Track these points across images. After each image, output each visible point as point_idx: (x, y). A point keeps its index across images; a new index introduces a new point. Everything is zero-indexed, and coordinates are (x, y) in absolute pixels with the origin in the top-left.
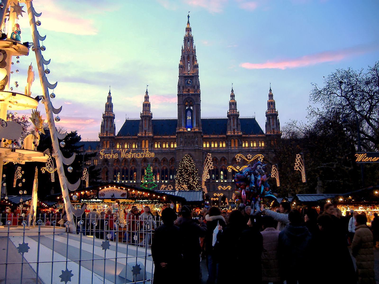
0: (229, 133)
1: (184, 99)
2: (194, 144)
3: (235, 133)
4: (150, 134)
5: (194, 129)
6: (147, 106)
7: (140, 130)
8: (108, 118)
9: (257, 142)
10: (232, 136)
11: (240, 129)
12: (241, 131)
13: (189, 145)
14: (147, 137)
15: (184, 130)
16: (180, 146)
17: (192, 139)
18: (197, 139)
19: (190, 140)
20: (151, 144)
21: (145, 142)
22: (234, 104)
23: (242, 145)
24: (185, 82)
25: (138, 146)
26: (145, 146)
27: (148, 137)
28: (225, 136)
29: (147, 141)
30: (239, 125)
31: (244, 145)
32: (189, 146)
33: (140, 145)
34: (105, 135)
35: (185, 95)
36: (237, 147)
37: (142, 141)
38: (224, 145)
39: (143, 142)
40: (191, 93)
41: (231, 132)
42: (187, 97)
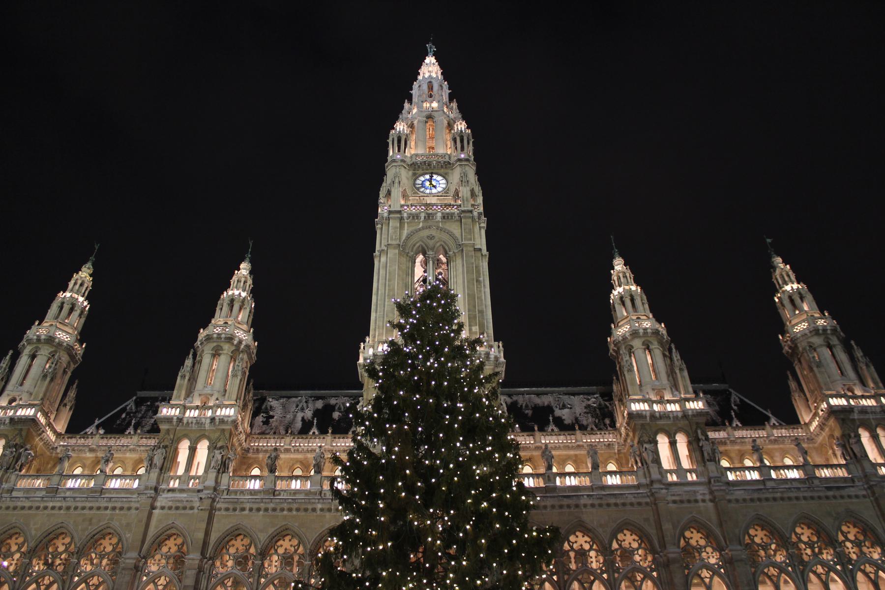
1: (405, 232)
7: (180, 390)
8: (40, 346)
14: (208, 421)
20: (219, 457)
21: (193, 450)
22: (635, 298)
24: (415, 180)
30: (681, 370)
33: (158, 460)
37: (179, 441)
42: (421, 225)
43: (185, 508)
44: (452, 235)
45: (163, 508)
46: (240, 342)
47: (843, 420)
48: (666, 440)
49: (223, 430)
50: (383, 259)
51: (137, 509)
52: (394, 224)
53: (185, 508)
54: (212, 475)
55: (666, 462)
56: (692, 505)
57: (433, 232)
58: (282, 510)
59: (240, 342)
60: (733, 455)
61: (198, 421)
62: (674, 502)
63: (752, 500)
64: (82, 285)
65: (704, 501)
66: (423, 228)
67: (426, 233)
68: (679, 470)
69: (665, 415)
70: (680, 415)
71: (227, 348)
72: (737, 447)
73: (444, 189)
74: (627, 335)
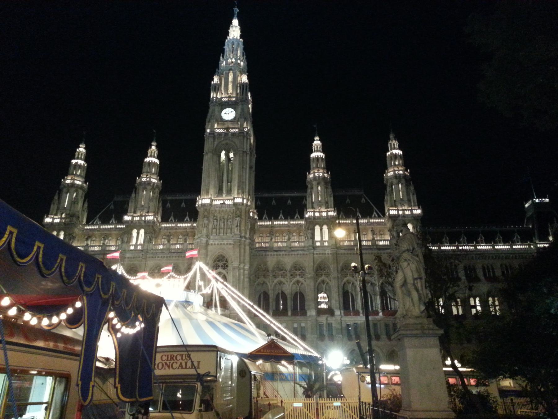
1: (216, 143)
2: (231, 230)
3: (322, 212)
5: (233, 200)
6: (152, 166)
12: (334, 208)
13: (222, 231)
14: (143, 222)
17: (227, 221)
18: (237, 219)
20: (148, 237)
21: (138, 234)
27: (145, 221)
29: (142, 232)
30: (330, 197)
32: (221, 234)
35: (220, 134)
37: (132, 230)
40: (231, 130)
41: (313, 210)
44: (235, 143)
45: (128, 258)
49: (149, 225)
52: (211, 140)
53: (136, 257)
55: (317, 238)
56: (324, 255)
57: (228, 141)
58: (173, 257)
61: (139, 221)
62: (317, 254)
63: (348, 254)
64: (82, 155)
65: (328, 254)
66: (223, 140)
68: (322, 241)
69: (319, 218)
70: (325, 218)
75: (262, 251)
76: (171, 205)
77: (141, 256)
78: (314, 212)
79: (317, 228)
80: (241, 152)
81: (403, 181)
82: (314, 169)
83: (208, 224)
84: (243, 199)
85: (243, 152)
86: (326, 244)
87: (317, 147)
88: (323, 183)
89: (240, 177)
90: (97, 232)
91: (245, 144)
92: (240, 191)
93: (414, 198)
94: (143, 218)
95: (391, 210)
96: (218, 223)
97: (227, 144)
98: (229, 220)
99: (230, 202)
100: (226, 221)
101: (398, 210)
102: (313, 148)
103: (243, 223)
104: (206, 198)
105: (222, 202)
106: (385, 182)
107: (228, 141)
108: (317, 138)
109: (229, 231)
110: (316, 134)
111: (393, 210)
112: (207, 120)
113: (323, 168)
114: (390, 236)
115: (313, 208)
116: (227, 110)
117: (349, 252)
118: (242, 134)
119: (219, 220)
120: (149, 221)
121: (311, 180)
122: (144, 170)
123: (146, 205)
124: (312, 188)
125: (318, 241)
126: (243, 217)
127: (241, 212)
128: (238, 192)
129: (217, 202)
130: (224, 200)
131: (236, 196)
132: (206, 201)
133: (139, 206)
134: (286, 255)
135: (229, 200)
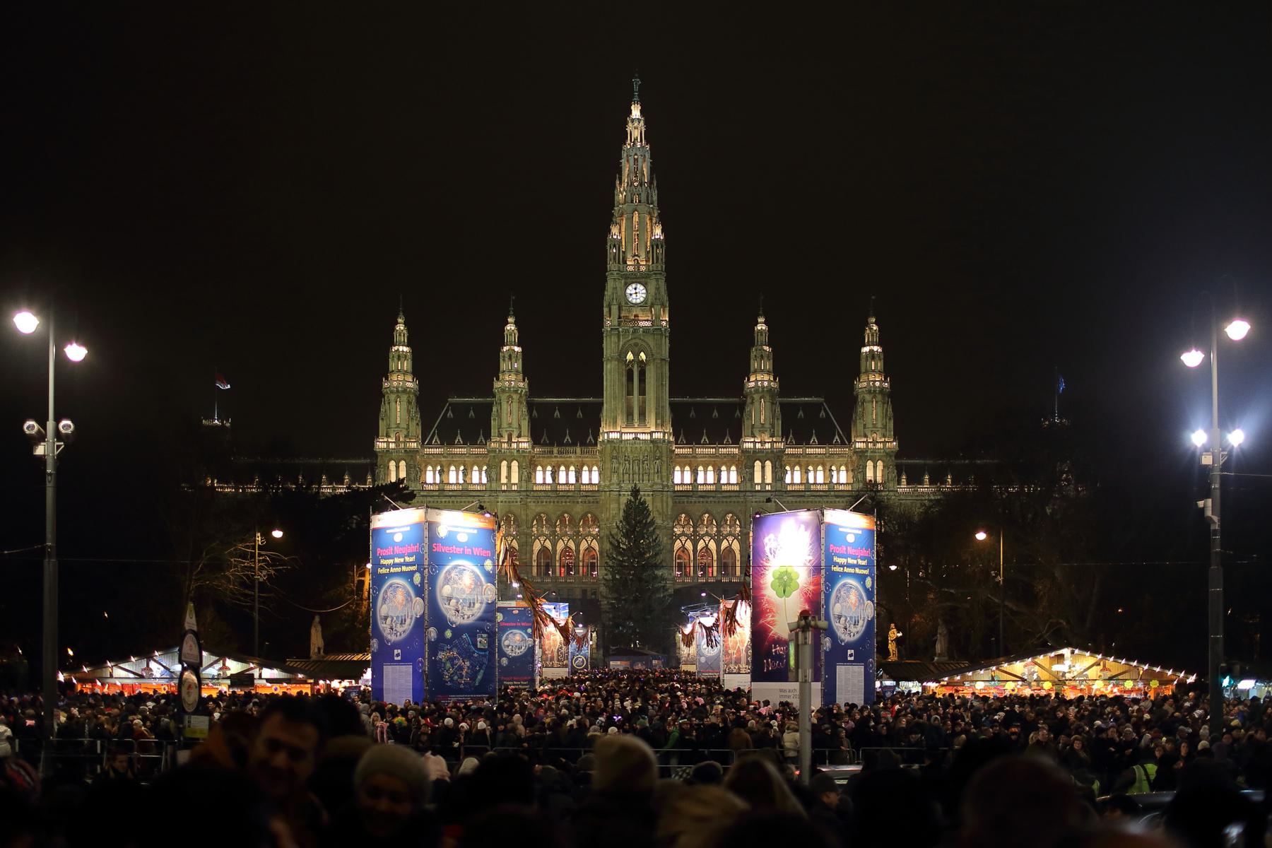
0: (748, 442)
1: (621, 343)
3: (766, 442)
4: (524, 442)
6: (513, 360)
8: (400, 394)
9: (828, 468)
10: (755, 451)
11: (780, 433)
14: (515, 451)
15: (621, 436)
16: (610, 481)
19: (638, 465)
21: (509, 467)
23: (782, 479)
25: (489, 476)
26: (509, 477)
28: (736, 451)
29: (515, 464)
30: (778, 419)
31: (788, 480)
34: (392, 446)
36: (770, 484)
38: (734, 478)
39: (504, 463)
41: (752, 440)
43: (513, 502)
45: (502, 502)
46: (522, 391)
47: (860, 456)
48: (760, 464)
50: (609, 366)
51: (488, 502)
52: (614, 339)
54: (524, 484)
55: (758, 479)
57: (637, 341)
58: (562, 502)
59: (522, 391)
60: (803, 464)
62: (756, 502)
63: (796, 502)
67: (633, 341)
68: (763, 483)
69: (761, 451)
70: (769, 451)
71: (515, 397)
72: (806, 459)
73: (645, 299)
74: (753, 390)
75: (683, 496)
76: (538, 413)
77: (519, 500)
78: (755, 443)
79: (758, 464)
80: (659, 361)
81: (879, 397)
82: (755, 372)
83: (618, 468)
84: (664, 433)
85: (662, 360)
86: (768, 488)
87: (761, 335)
88: (768, 397)
89: (658, 399)
90: (443, 459)
91: (663, 348)
92: (659, 421)
93: (891, 425)
94: (514, 446)
95: (858, 442)
96: (631, 467)
97: (636, 345)
98: (646, 462)
99: (647, 437)
100: (641, 461)
101: (867, 442)
102: (756, 335)
103: (664, 467)
104: (614, 432)
105: (633, 436)
106: (855, 393)
107: (637, 341)
108: (761, 320)
109: (646, 477)
110: (761, 312)
111: (861, 442)
112: (605, 305)
113: (768, 373)
114: (853, 478)
115: (754, 436)
116: (630, 290)
117: (798, 500)
118: (654, 331)
119: (631, 461)
120: (524, 450)
121: (751, 392)
122: (504, 366)
123: (515, 425)
124: (752, 403)
125: (758, 484)
126: (664, 459)
127: (661, 452)
128: (656, 422)
129: (631, 437)
130: (637, 433)
131: (653, 429)
132: (614, 436)
133: (504, 425)
134: (715, 502)
135: (645, 433)
